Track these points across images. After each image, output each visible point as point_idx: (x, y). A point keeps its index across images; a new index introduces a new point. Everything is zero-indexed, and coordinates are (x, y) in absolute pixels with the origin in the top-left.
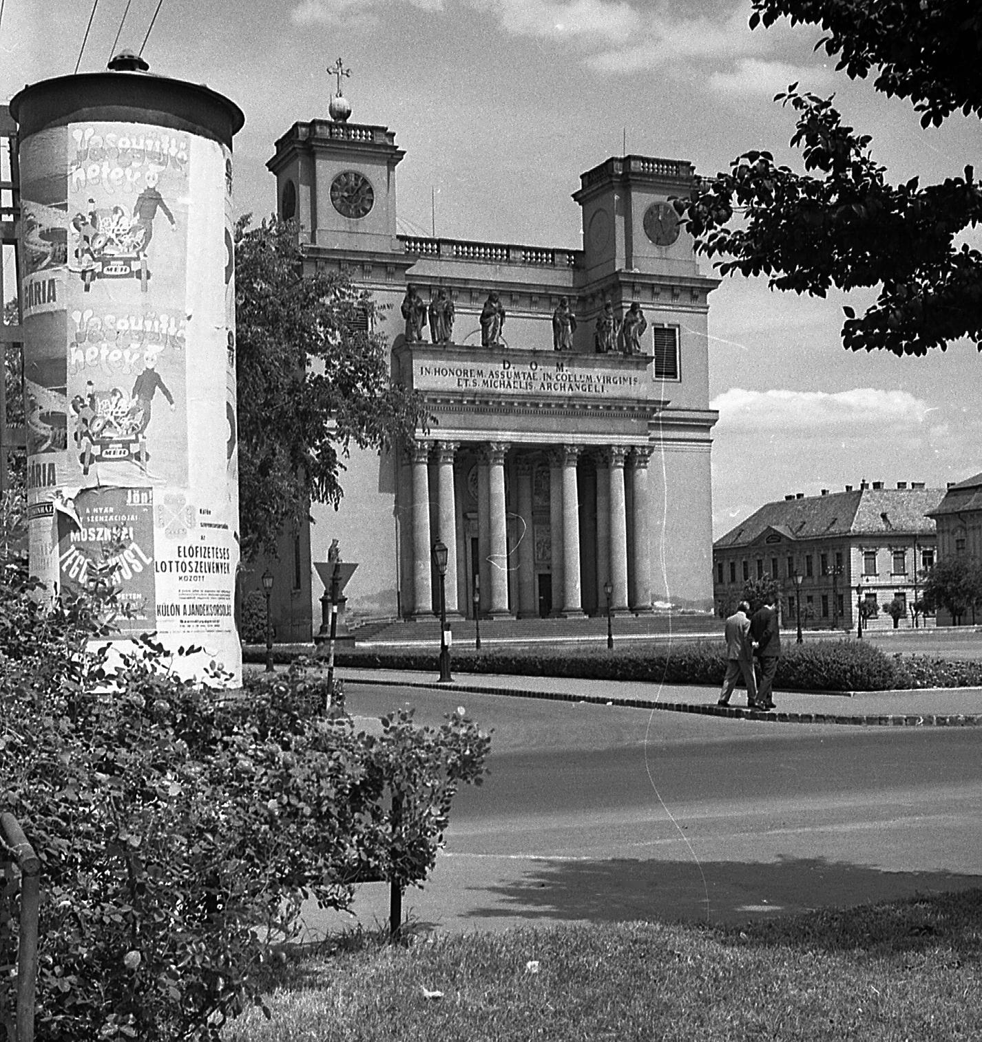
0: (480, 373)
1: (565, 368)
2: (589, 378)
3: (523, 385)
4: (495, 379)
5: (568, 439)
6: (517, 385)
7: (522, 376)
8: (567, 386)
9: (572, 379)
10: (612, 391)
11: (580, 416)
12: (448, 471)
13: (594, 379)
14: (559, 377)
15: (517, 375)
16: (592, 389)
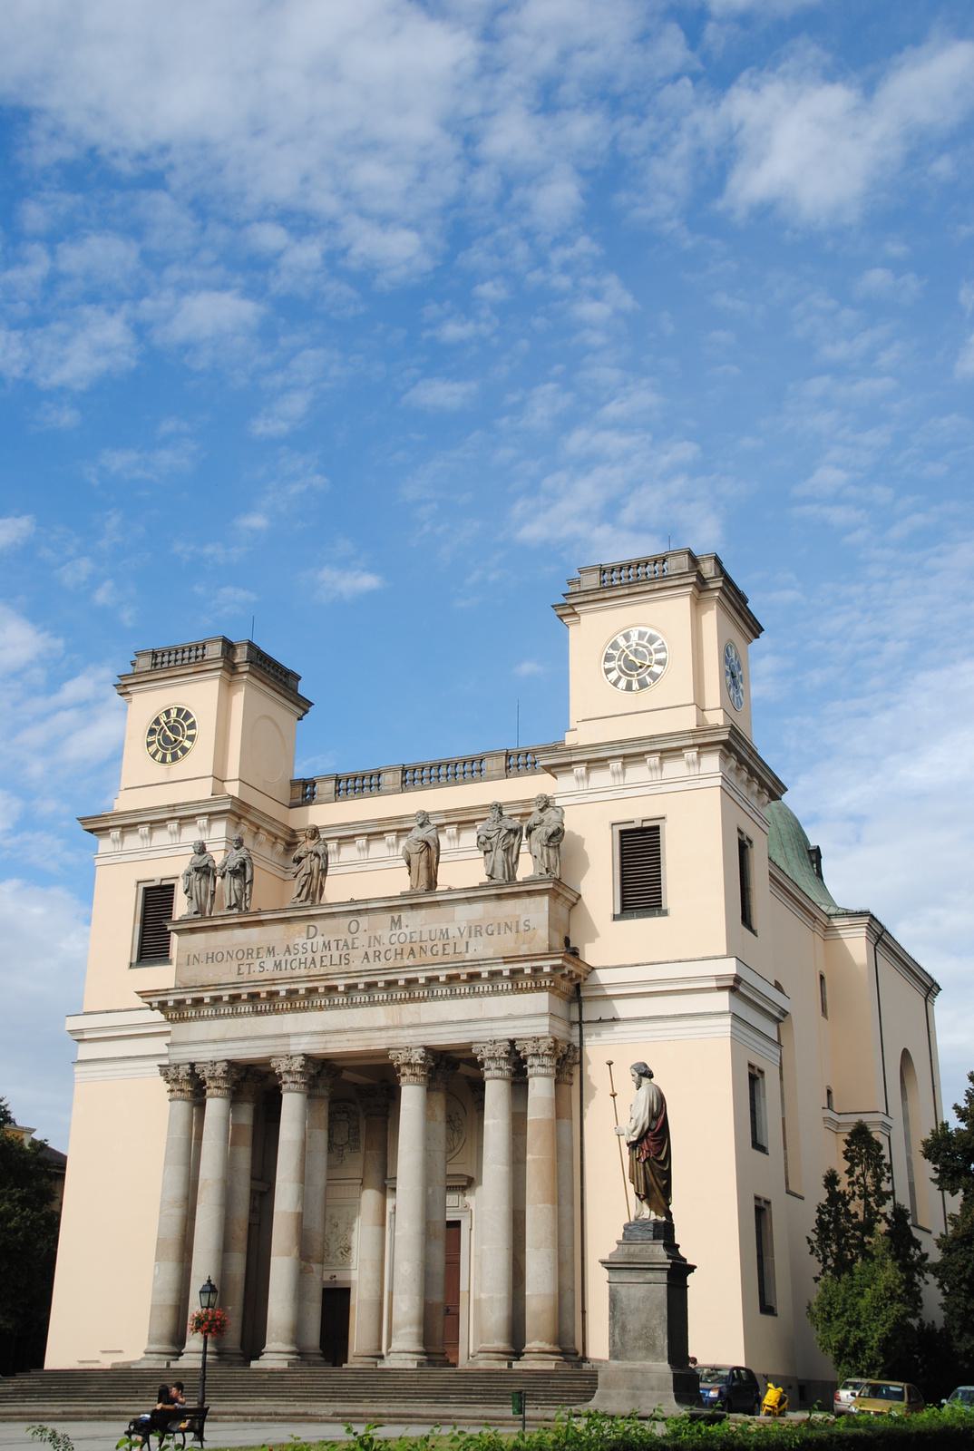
0: (271, 951)
2: (445, 934)
3: (336, 960)
4: (290, 958)
7: (333, 945)
8: (407, 950)
9: (416, 937)
10: (483, 950)
13: (453, 932)
14: (394, 939)
15: (327, 946)
16: (450, 950)
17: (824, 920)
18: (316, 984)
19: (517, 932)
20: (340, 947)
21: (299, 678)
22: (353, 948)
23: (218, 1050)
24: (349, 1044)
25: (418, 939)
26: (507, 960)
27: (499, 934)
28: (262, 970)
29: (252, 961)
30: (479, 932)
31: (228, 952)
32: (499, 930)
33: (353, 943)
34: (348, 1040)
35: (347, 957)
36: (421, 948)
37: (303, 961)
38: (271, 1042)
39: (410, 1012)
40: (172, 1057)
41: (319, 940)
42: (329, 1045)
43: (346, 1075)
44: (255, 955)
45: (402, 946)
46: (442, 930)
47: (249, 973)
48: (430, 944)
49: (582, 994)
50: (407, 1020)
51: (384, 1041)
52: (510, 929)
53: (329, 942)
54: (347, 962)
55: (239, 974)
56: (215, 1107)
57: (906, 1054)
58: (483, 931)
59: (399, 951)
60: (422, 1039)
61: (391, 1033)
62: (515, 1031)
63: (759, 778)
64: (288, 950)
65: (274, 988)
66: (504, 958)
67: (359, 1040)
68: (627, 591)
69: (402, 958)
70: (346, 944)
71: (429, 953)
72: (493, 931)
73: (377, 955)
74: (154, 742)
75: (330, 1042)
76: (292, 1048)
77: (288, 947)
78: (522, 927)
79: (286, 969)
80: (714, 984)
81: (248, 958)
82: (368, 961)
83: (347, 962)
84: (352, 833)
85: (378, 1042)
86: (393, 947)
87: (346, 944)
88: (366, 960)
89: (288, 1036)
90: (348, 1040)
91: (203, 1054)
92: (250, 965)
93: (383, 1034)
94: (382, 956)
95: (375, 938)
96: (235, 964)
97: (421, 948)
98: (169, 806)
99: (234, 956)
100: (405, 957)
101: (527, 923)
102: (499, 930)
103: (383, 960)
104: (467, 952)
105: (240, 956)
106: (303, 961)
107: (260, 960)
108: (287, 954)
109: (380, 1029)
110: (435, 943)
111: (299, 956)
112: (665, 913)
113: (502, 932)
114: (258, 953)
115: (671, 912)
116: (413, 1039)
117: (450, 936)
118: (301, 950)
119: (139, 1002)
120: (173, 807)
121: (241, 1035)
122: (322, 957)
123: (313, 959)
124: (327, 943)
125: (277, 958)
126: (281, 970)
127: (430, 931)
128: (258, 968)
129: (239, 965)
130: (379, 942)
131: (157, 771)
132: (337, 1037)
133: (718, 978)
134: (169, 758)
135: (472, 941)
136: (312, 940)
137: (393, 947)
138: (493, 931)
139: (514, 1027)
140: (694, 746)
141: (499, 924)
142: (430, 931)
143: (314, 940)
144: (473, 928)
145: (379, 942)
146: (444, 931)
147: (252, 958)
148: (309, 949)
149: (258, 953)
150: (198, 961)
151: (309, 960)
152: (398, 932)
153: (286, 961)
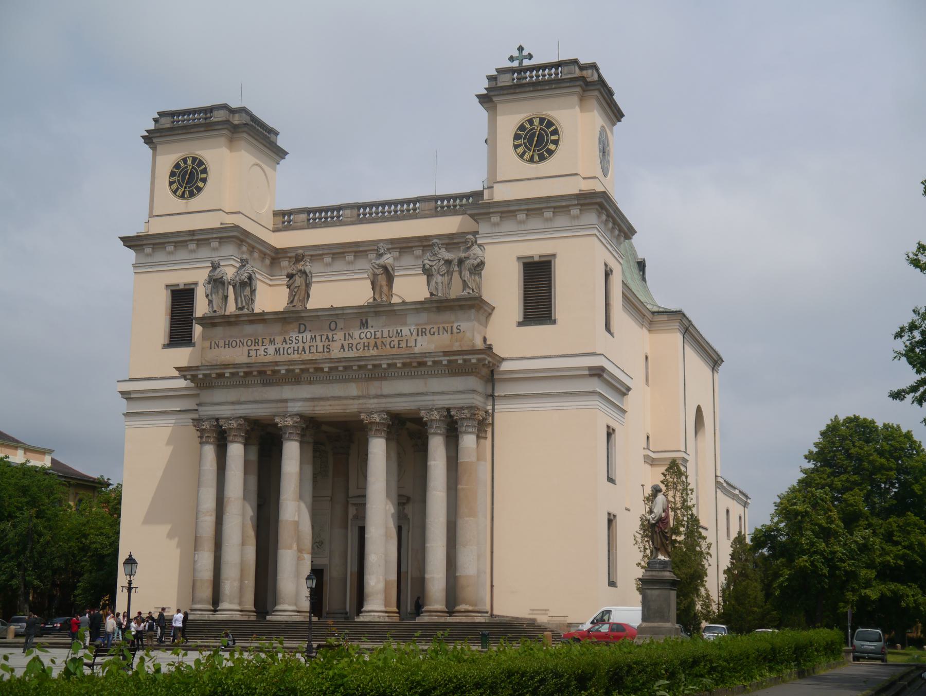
0: (272, 341)
1: (370, 323)
2: (399, 333)
3: (320, 349)
4: (288, 346)
5: (372, 404)
6: (313, 350)
7: (318, 338)
8: (372, 344)
9: (379, 335)
10: (425, 345)
11: (383, 378)
12: (236, 450)
13: (405, 331)
14: (363, 335)
15: (313, 339)
16: (403, 344)
17: (649, 316)
18: (308, 366)
19: (452, 333)
20: (323, 340)
21: (277, 134)
22: (333, 341)
23: (234, 410)
24: (331, 408)
25: (380, 336)
26: (446, 354)
27: (439, 334)
28: (265, 354)
29: (257, 347)
30: (424, 333)
31: (240, 341)
32: (439, 332)
33: (333, 338)
34: (330, 405)
35: (328, 347)
36: (382, 342)
37: (296, 349)
38: (274, 405)
39: (374, 388)
40: (201, 413)
41: (307, 335)
42: (317, 408)
43: (324, 428)
44: (260, 344)
45: (368, 340)
46: (397, 330)
47: (256, 356)
48: (389, 340)
49: (496, 377)
50: (373, 391)
51: (356, 406)
52: (447, 332)
53: (315, 337)
54: (328, 350)
55: (249, 356)
56: (236, 450)
57: (699, 410)
58: (427, 332)
59: (366, 344)
60: (383, 405)
61: (361, 401)
62: (450, 402)
63: (619, 225)
64: (285, 341)
65: (276, 368)
66: (443, 352)
67: (338, 405)
68: (532, 89)
69: (369, 349)
70: (328, 338)
71: (388, 346)
72: (434, 332)
73: (350, 347)
74: (174, 182)
75: (317, 406)
76: (289, 409)
77: (285, 338)
78: (455, 330)
79: (284, 354)
80: (587, 372)
81: (255, 346)
82: (344, 351)
83: (328, 350)
84: (321, 252)
85: (352, 407)
86: (362, 341)
87: (328, 338)
88: (342, 350)
89: (286, 401)
90: (330, 405)
91: (225, 411)
92: (256, 350)
93: (356, 402)
94: (354, 346)
95: (349, 334)
96: (246, 348)
97: (382, 342)
98: (189, 231)
99: (245, 344)
100: (371, 348)
101: (459, 327)
102: (439, 332)
103: (355, 350)
104: (416, 346)
105: (249, 343)
106: (296, 349)
107: (265, 347)
108: (284, 343)
109: (354, 398)
110: (392, 339)
111: (293, 345)
112: (554, 322)
113: (441, 333)
114: (263, 342)
115: (558, 321)
116: (377, 406)
117: (404, 334)
118: (294, 339)
119: (176, 373)
120: (192, 233)
121: (252, 399)
122: (310, 346)
123: (304, 347)
124: (313, 337)
125: (277, 346)
126: (280, 355)
127: (389, 331)
128: (263, 353)
129: (249, 350)
130: (352, 338)
131: (180, 205)
132: (322, 403)
133: (590, 368)
134: (187, 194)
135: (419, 339)
136: (302, 335)
137: (362, 341)
138: (434, 332)
139: (450, 399)
140: (577, 205)
141: (439, 328)
142: (389, 331)
143: (304, 335)
144: (420, 330)
145: (352, 338)
146: (399, 331)
147: (258, 345)
148: (300, 339)
149: (263, 342)
150: (218, 346)
151: (301, 348)
152: (366, 331)
153: (284, 348)
